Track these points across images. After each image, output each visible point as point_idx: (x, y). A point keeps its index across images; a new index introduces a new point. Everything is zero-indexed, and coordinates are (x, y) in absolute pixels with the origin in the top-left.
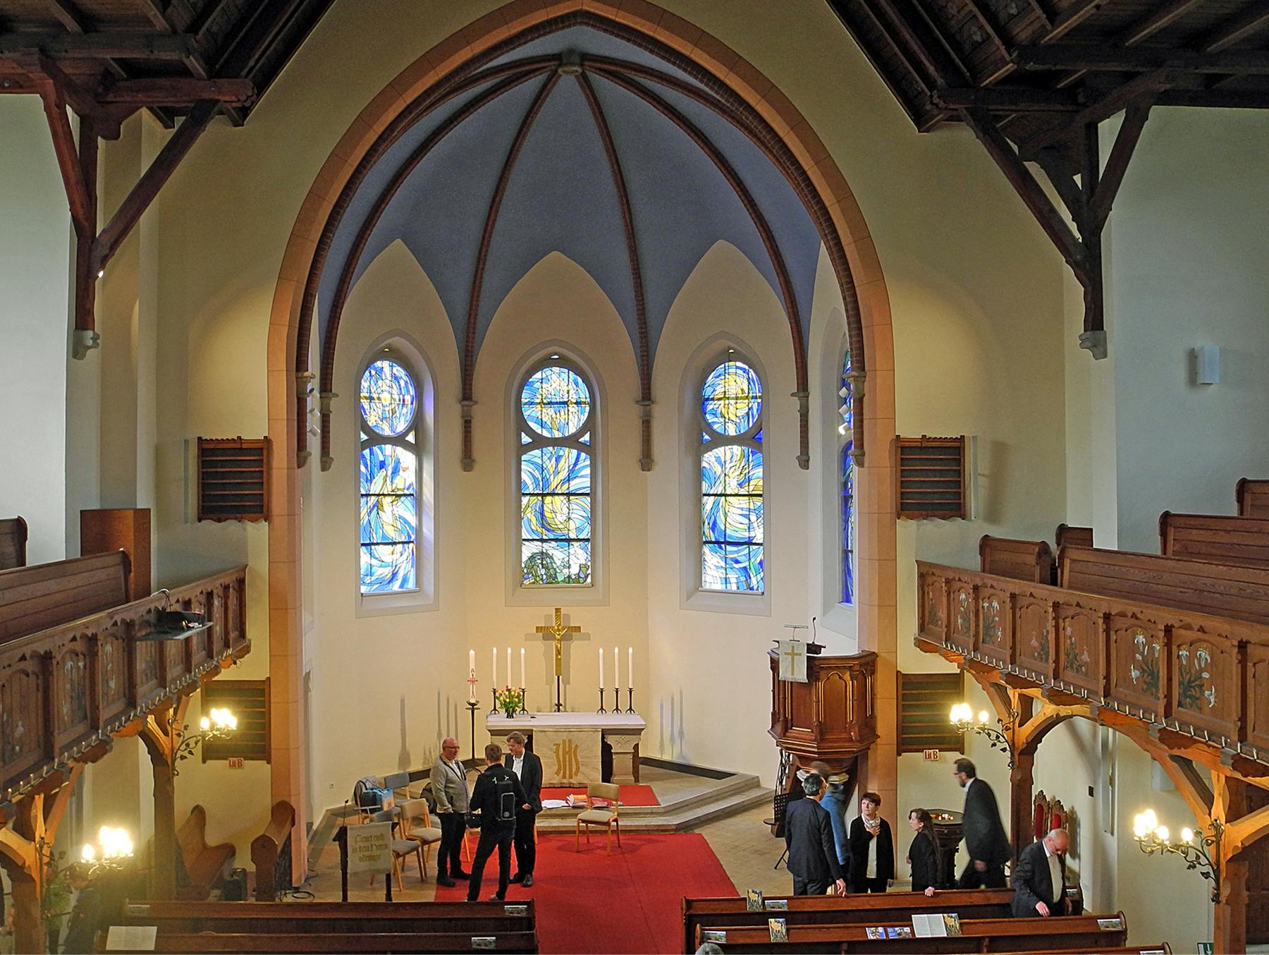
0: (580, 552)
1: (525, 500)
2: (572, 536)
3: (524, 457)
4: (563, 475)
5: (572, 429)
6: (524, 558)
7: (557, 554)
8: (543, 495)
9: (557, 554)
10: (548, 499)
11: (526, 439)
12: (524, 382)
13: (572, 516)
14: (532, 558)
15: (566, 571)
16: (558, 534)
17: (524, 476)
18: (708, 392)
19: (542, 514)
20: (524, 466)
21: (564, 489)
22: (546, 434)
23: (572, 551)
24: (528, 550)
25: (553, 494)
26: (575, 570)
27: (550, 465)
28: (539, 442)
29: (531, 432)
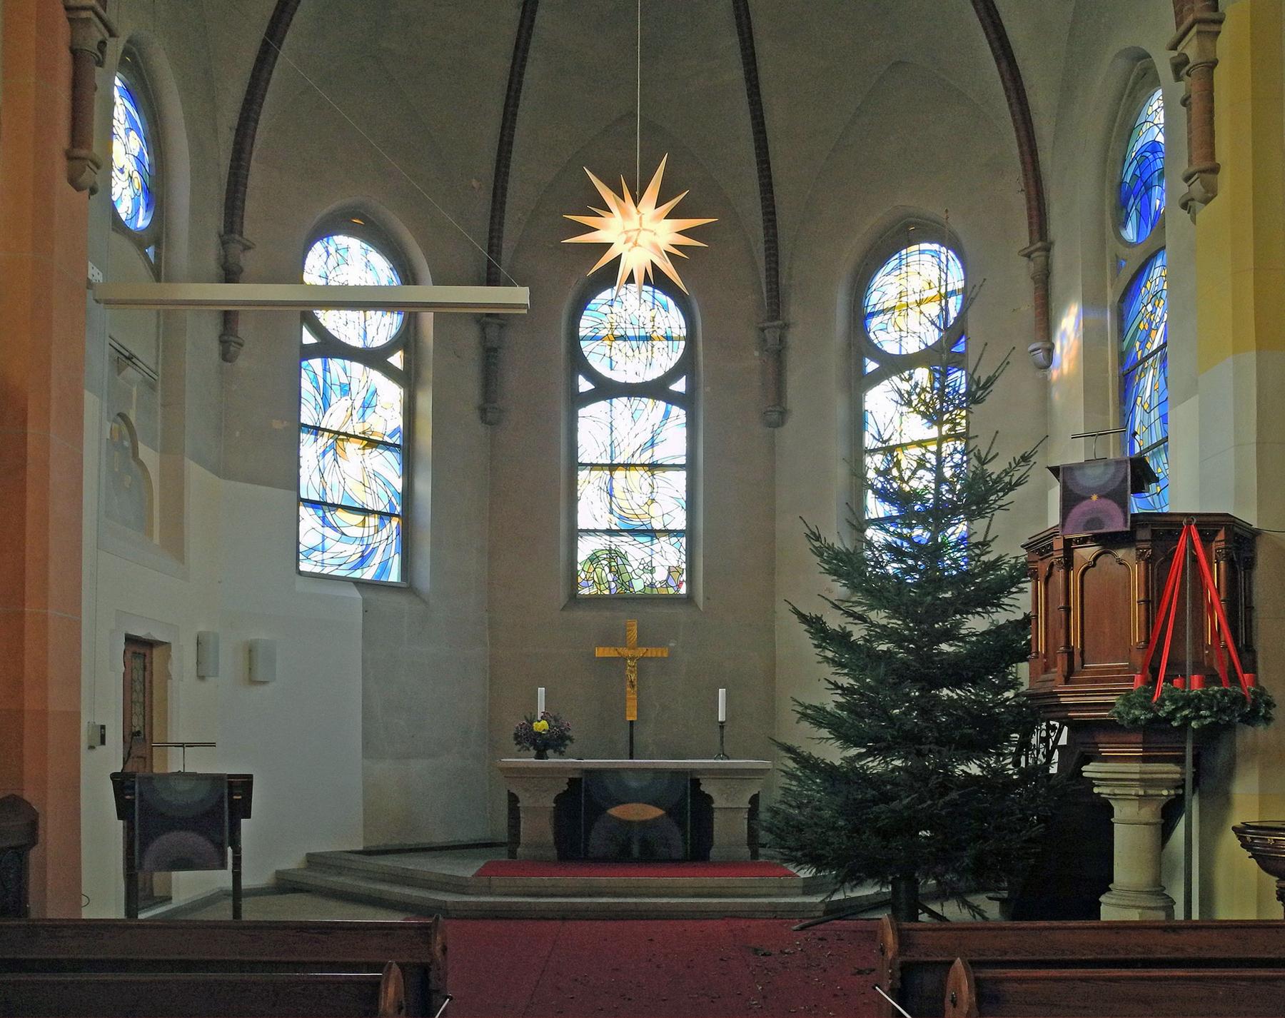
0: (667, 547)
2: (657, 525)
3: (582, 412)
8: (612, 467)
9: (634, 550)
10: (619, 474)
11: (585, 385)
14: (594, 559)
15: (647, 577)
16: (636, 523)
18: (874, 299)
21: (645, 458)
23: (657, 547)
24: (586, 547)
25: (627, 466)
26: (661, 575)
27: (623, 424)
28: (607, 390)
29: (592, 375)
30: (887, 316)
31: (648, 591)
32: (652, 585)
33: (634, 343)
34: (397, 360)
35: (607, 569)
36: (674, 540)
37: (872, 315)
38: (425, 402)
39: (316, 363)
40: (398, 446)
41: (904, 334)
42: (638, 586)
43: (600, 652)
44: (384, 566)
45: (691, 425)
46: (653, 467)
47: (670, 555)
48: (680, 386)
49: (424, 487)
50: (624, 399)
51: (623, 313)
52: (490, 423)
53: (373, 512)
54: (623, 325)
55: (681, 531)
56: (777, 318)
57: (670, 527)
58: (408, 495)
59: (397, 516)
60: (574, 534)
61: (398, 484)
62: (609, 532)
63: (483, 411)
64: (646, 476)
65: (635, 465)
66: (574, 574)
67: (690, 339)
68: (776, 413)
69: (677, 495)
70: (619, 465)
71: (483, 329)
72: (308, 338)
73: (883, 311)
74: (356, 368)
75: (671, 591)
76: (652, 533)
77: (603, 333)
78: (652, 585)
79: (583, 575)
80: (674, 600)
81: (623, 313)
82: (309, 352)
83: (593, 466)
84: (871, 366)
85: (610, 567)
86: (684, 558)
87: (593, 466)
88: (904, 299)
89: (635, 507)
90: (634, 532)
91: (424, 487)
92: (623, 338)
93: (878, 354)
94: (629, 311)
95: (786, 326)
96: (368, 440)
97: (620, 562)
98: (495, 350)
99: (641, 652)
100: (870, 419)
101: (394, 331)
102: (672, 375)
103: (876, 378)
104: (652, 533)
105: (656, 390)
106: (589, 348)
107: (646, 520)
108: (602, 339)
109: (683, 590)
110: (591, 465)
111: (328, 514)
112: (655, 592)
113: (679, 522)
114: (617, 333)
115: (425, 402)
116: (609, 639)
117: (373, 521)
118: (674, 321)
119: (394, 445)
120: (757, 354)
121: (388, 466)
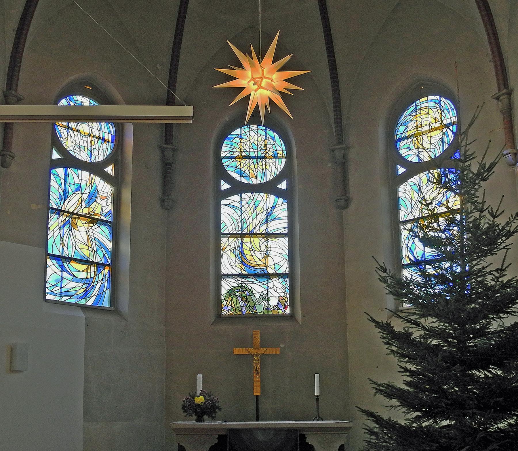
1: (224, 240)
2: (271, 271)
4: (263, 216)
5: (269, 177)
6: (224, 291)
7: (257, 288)
8: (242, 235)
9: (257, 288)
10: (246, 240)
11: (225, 186)
12: (224, 136)
13: (271, 253)
14: (231, 292)
16: (258, 270)
17: (223, 218)
19: (242, 253)
20: (225, 211)
21: (263, 229)
22: (244, 180)
23: (271, 285)
24: (226, 286)
25: (252, 234)
26: (273, 302)
29: (229, 179)
30: (410, 140)
31: (266, 312)
32: (268, 309)
33: (255, 160)
34: (110, 170)
35: (240, 299)
36: (281, 280)
37: (401, 140)
38: (127, 195)
39: (60, 171)
40: (110, 222)
41: (421, 150)
42: (259, 310)
43: (237, 351)
44: (100, 296)
45: (291, 210)
46: (268, 235)
47: (278, 289)
48: (283, 185)
49: (125, 248)
50: (249, 194)
51: (248, 143)
52: (166, 209)
53: (93, 263)
54: (248, 150)
55: (286, 274)
56: (342, 143)
57: (279, 272)
58: (115, 253)
59: (109, 265)
60: (220, 277)
61: (109, 245)
62: (241, 276)
63: (163, 201)
64: (263, 240)
65: (256, 234)
66: (219, 302)
67: (289, 157)
68: (344, 201)
69: (283, 252)
70: (247, 234)
71: (163, 152)
72: (56, 155)
73: (407, 138)
74: (85, 175)
75: (280, 312)
76: (268, 276)
77: (237, 154)
78: (268, 309)
79: (225, 303)
80: (283, 317)
81: (248, 143)
82: (56, 164)
83: (231, 235)
84: (401, 170)
85: (242, 298)
86: (288, 291)
87: (231, 235)
88: (420, 129)
89: (257, 259)
90: (256, 276)
91: (125, 248)
92: (248, 157)
93: (404, 162)
94: (252, 141)
95: (348, 148)
96: (92, 218)
97: (248, 294)
98: (170, 164)
99: (262, 351)
100: (402, 202)
101: (109, 153)
102: (278, 179)
103: (405, 177)
104: (268, 276)
105: (269, 188)
106: (227, 164)
107: (264, 268)
108: (235, 158)
109: (288, 311)
110: (229, 234)
111: (65, 264)
112: (270, 312)
113: (284, 268)
114: (244, 154)
115: (127, 195)
116: (242, 344)
117: (93, 269)
118: (279, 146)
119: (107, 222)
120: (330, 165)
121: (103, 234)
